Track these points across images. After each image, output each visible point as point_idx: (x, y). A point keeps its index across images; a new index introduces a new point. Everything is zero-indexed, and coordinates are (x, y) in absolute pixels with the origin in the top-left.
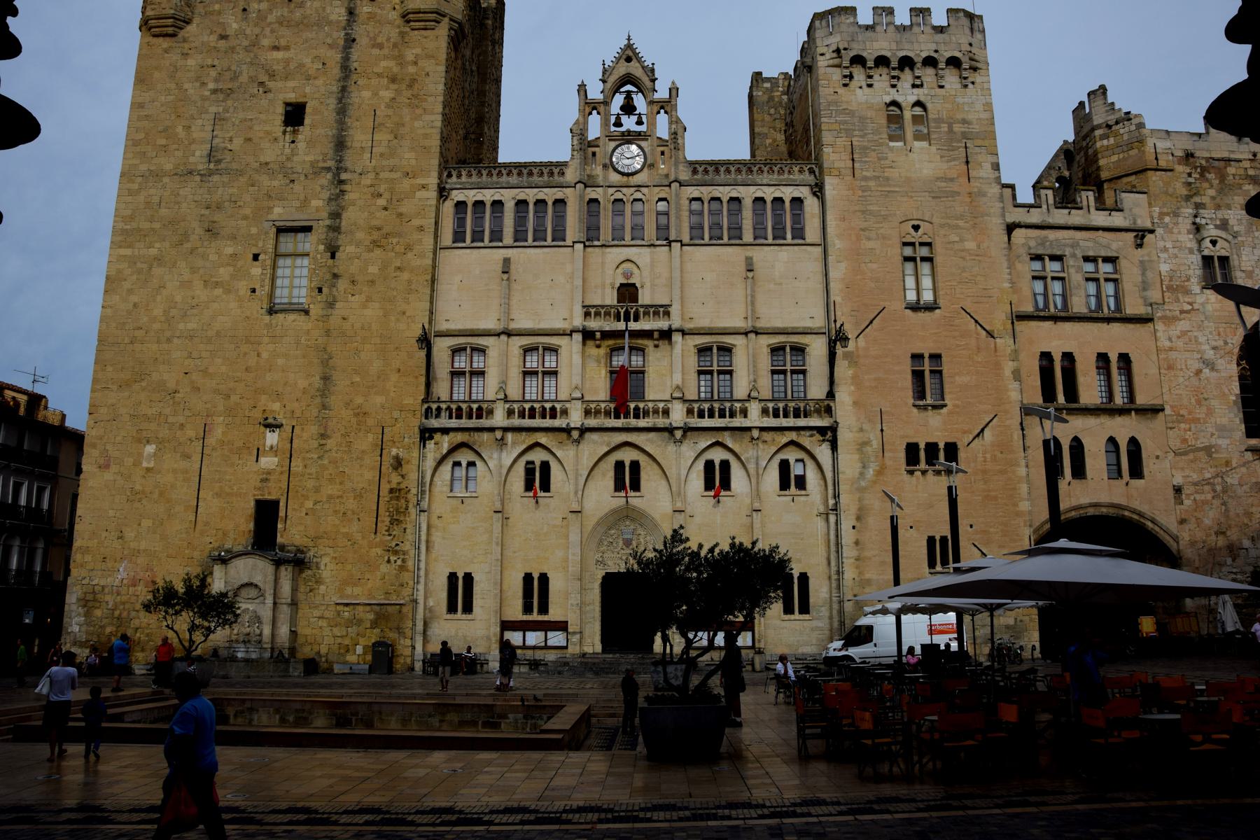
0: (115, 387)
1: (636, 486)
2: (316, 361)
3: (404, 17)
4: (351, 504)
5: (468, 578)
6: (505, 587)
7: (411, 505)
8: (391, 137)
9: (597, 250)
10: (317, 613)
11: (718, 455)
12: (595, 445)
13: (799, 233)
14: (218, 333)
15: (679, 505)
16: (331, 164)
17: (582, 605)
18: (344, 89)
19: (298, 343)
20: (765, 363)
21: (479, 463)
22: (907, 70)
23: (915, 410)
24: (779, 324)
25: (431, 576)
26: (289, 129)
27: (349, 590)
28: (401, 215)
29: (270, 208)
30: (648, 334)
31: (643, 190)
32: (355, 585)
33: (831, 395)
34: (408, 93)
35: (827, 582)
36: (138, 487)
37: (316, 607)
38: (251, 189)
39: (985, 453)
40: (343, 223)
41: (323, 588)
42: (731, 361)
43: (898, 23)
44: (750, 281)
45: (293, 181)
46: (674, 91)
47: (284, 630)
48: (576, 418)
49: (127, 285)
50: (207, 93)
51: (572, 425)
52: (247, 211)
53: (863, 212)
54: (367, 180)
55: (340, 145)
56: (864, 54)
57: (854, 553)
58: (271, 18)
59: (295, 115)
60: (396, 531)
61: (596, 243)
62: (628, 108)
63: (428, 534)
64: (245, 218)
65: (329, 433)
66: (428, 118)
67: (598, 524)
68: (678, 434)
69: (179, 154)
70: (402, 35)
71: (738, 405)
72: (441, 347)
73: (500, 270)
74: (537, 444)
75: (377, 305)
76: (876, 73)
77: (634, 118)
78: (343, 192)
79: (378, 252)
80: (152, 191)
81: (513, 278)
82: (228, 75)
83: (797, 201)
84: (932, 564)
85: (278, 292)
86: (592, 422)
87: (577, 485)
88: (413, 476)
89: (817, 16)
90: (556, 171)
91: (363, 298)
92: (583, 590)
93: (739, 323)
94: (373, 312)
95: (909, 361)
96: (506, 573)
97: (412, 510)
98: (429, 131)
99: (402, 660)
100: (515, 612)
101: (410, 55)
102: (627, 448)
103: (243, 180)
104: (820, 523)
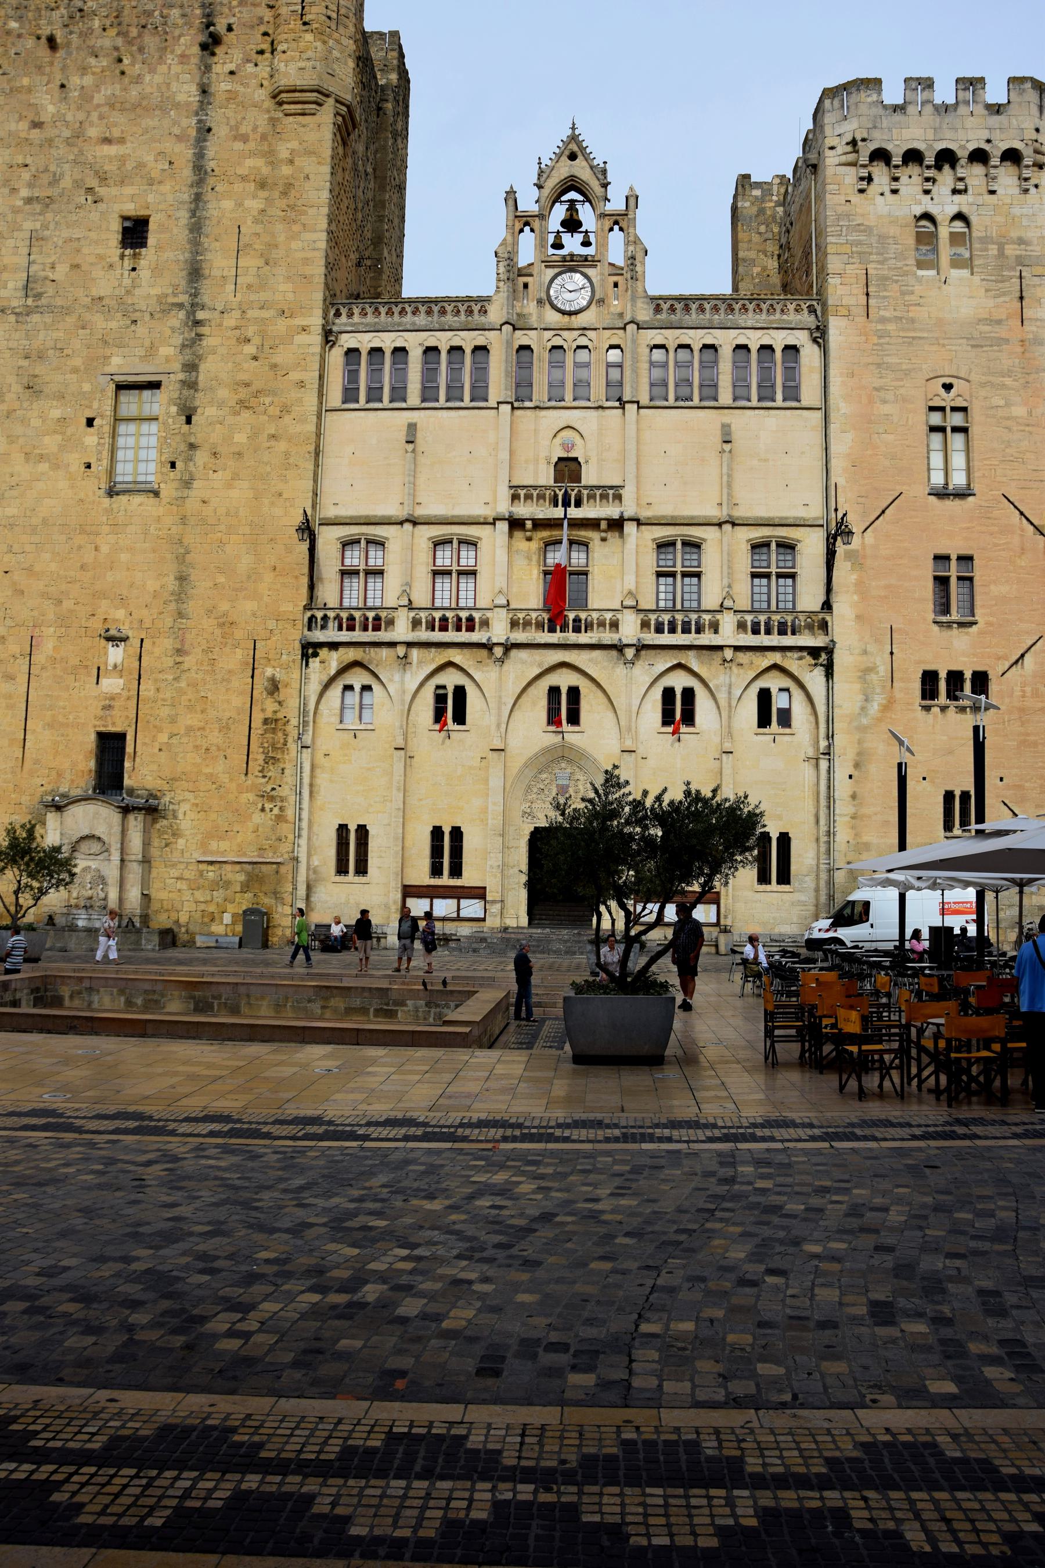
1: (574, 718)
2: (169, 556)
3: (274, 97)
4: (215, 737)
5: (363, 831)
6: (407, 844)
7: (290, 740)
8: (260, 262)
9: (528, 412)
10: (174, 873)
11: (679, 681)
12: (524, 665)
13: (792, 393)
14: (45, 521)
15: (629, 744)
16: (184, 298)
17: (504, 867)
18: (198, 198)
20: (744, 563)
21: (376, 687)
22: (947, 168)
23: (936, 628)
24: (761, 512)
25: (315, 828)
26: (128, 252)
27: (214, 845)
28: (274, 367)
29: (106, 358)
30: (593, 524)
31: (588, 333)
32: (221, 838)
33: (827, 606)
34: (282, 203)
35: (814, 845)
37: (174, 866)
38: (81, 331)
39: (1024, 684)
40: (201, 378)
41: (181, 842)
42: (699, 560)
43: (938, 101)
44: (726, 455)
46: (632, 200)
47: (134, 895)
48: (499, 631)
50: (20, 203)
51: (495, 641)
52: (77, 362)
53: (879, 365)
54: (230, 321)
55: (195, 273)
56: (889, 147)
57: (851, 810)
59: (135, 233)
60: (273, 772)
61: (527, 404)
62: (572, 224)
63: (312, 776)
64: (75, 370)
65: (186, 647)
66: (308, 236)
67: (526, 765)
68: (630, 653)
70: (273, 121)
71: (707, 617)
72: (328, 539)
73: (404, 439)
74: (450, 664)
76: (903, 173)
77: (579, 237)
78: (199, 336)
79: (246, 414)
81: (420, 449)
82: (45, 178)
83: (792, 349)
84: (948, 826)
85: (120, 468)
86: (520, 636)
87: (499, 715)
88: (293, 704)
89: (828, 93)
90: (476, 308)
91: (228, 475)
92: (505, 848)
93: (712, 512)
94: (240, 493)
95: (930, 563)
96: (409, 827)
97: (292, 746)
98: (310, 254)
99: (279, 932)
100: (421, 874)
102: (564, 670)
103: (71, 320)
104: (808, 770)
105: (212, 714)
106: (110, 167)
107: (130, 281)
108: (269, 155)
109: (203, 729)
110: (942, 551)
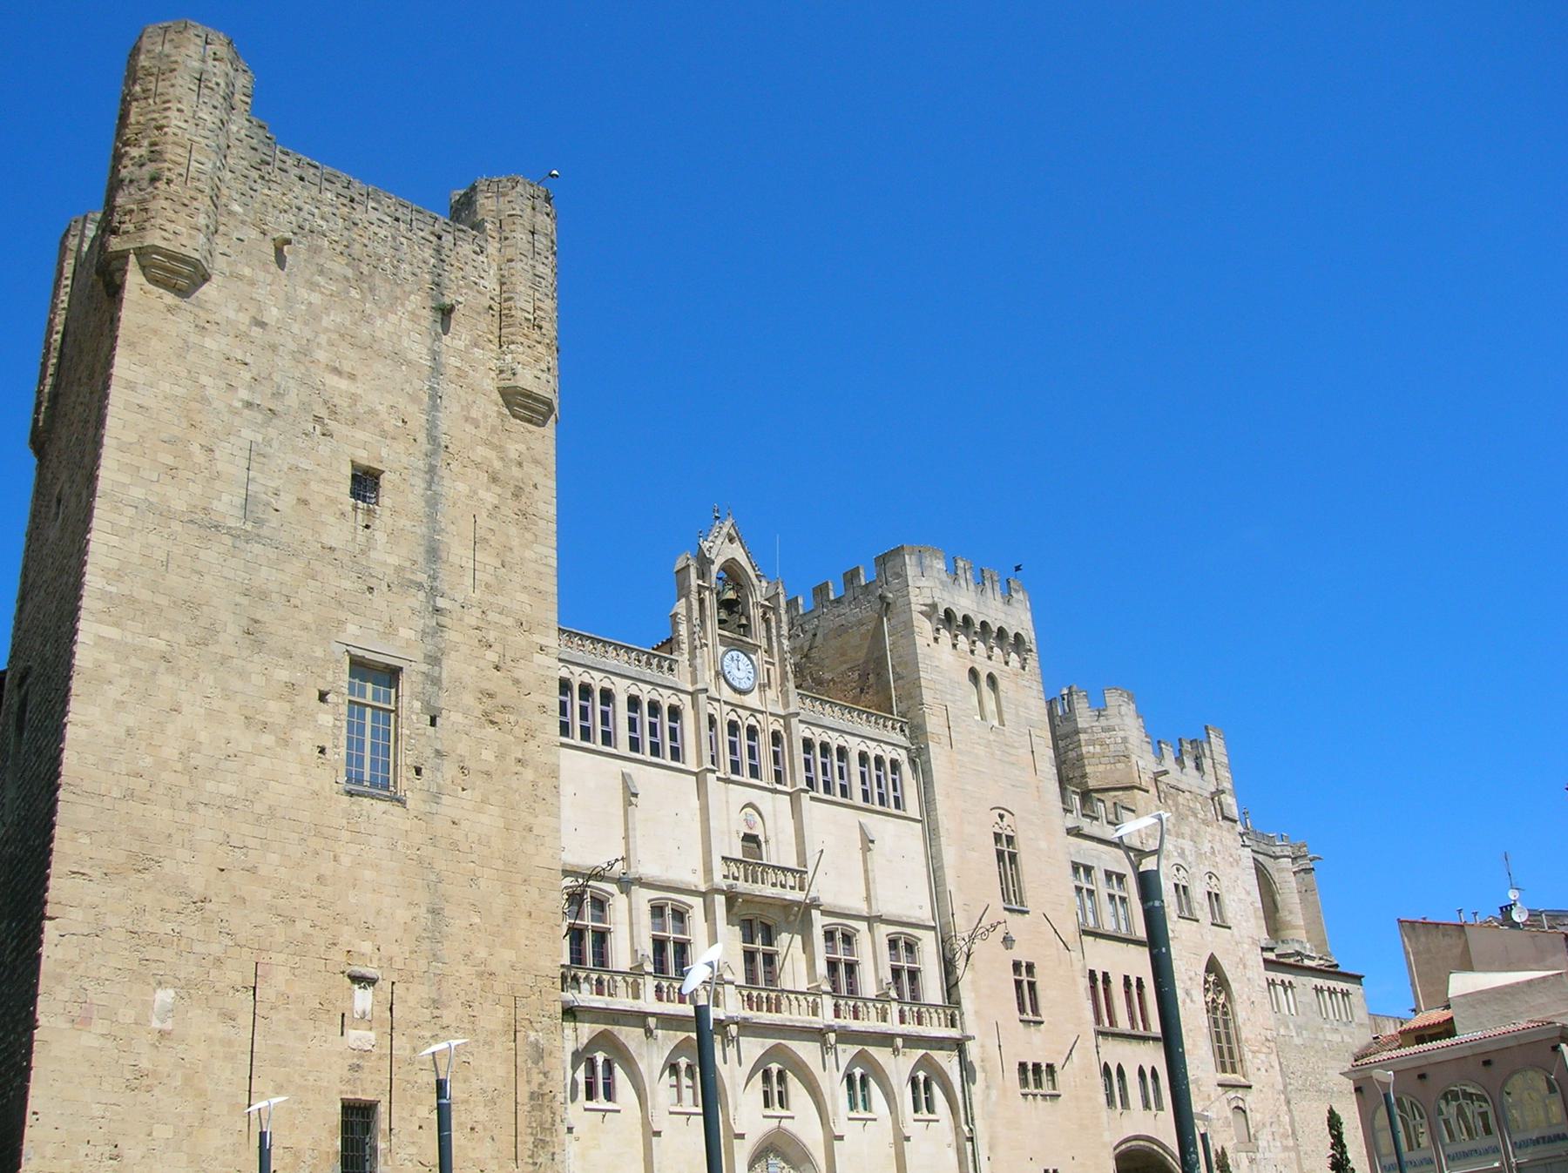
0: (97, 874)
7: (558, 1119)
16: (422, 577)
18: (432, 470)
19: (393, 847)
28: (516, 682)
36: (145, 1064)
40: (444, 675)
45: (371, 589)
49: (114, 692)
50: (239, 405)
52: (308, 617)
58: (326, 321)
59: (365, 483)
64: (306, 628)
69: (196, 489)
75: (495, 810)
79: (491, 730)
80: (153, 539)
101: (514, 449)
103: (297, 566)
105: (476, 1084)
106: (343, 403)
107: (363, 539)
108: (500, 449)
109: (467, 1101)
110: (1018, 959)
